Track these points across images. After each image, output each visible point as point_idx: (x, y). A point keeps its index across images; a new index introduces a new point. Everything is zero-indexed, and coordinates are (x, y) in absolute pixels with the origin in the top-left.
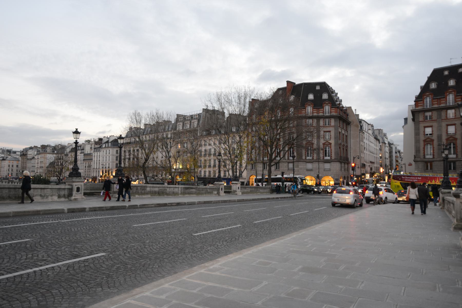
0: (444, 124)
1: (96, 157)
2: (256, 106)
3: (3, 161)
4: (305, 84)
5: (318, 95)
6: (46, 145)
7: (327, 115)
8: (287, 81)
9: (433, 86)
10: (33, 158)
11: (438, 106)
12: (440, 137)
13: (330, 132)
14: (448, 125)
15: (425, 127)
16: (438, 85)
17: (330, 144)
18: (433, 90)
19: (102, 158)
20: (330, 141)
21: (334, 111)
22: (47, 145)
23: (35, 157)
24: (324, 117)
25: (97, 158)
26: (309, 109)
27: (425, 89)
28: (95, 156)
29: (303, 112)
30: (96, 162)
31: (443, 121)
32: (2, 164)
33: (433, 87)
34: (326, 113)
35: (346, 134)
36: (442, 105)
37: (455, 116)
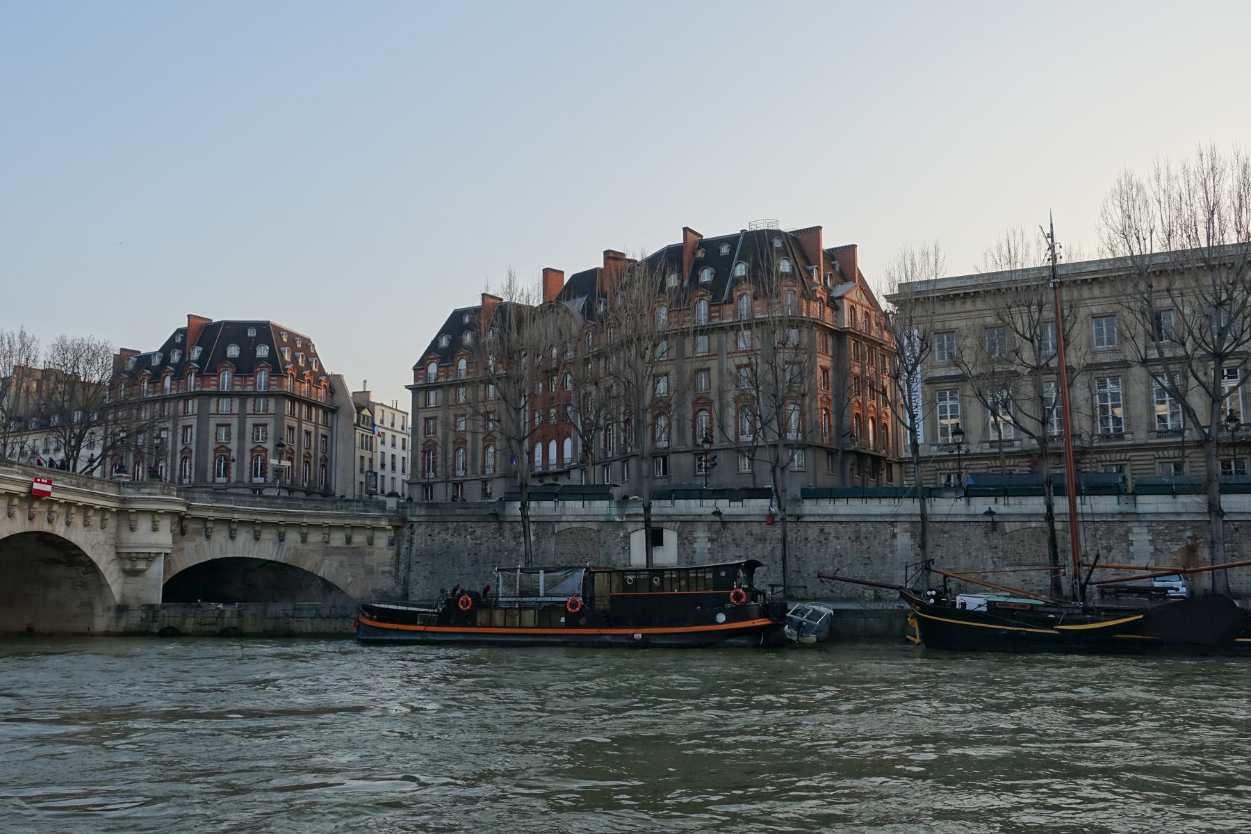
2: (130, 364)
4: (227, 323)
5: (248, 349)
7: (263, 390)
9: (444, 343)
17: (266, 451)
18: (443, 349)
20: (265, 446)
21: (275, 382)
24: (256, 396)
26: (226, 377)
29: (212, 383)
34: (260, 386)
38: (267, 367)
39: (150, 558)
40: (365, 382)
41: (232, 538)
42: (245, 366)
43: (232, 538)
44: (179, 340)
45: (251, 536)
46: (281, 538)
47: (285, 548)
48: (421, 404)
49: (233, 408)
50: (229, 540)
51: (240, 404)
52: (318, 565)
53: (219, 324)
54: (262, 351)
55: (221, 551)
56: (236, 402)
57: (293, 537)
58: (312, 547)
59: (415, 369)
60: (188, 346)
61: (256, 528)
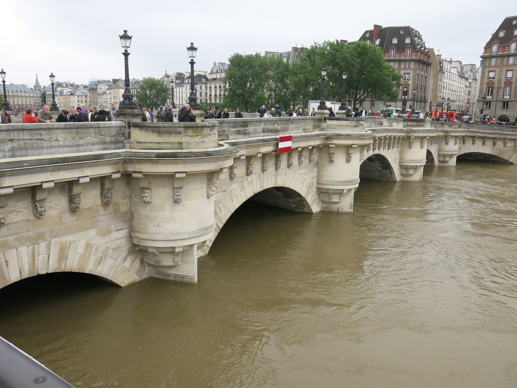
0: (504, 69)
1: (178, 93)
3: (72, 96)
6: (117, 79)
8: (374, 25)
9: (502, 34)
10: (105, 93)
11: (502, 53)
12: (500, 81)
13: (409, 74)
14: (507, 71)
15: (489, 72)
16: (506, 34)
17: (409, 85)
18: (501, 38)
19: (185, 94)
20: (408, 83)
22: (118, 80)
23: (107, 91)
24: (405, 61)
25: (179, 94)
27: (495, 36)
28: (176, 92)
29: (386, 55)
30: (178, 98)
31: (504, 66)
32: (71, 99)
33: (501, 35)
35: (426, 75)
36: (506, 53)
37: (514, 63)
38: (411, 47)
39: (451, 156)
40: (439, 50)
41: (473, 144)
42: (401, 47)
43: (473, 144)
44: (368, 36)
45: (481, 143)
46: (494, 144)
47: (496, 148)
48: (487, 64)
49: (395, 66)
50: (472, 145)
51: (398, 64)
52: (511, 156)
53: (386, 29)
54: (408, 41)
55: (468, 149)
56: (397, 64)
57: (500, 144)
58: (508, 148)
59: (485, 48)
60: (374, 39)
61: (484, 139)
